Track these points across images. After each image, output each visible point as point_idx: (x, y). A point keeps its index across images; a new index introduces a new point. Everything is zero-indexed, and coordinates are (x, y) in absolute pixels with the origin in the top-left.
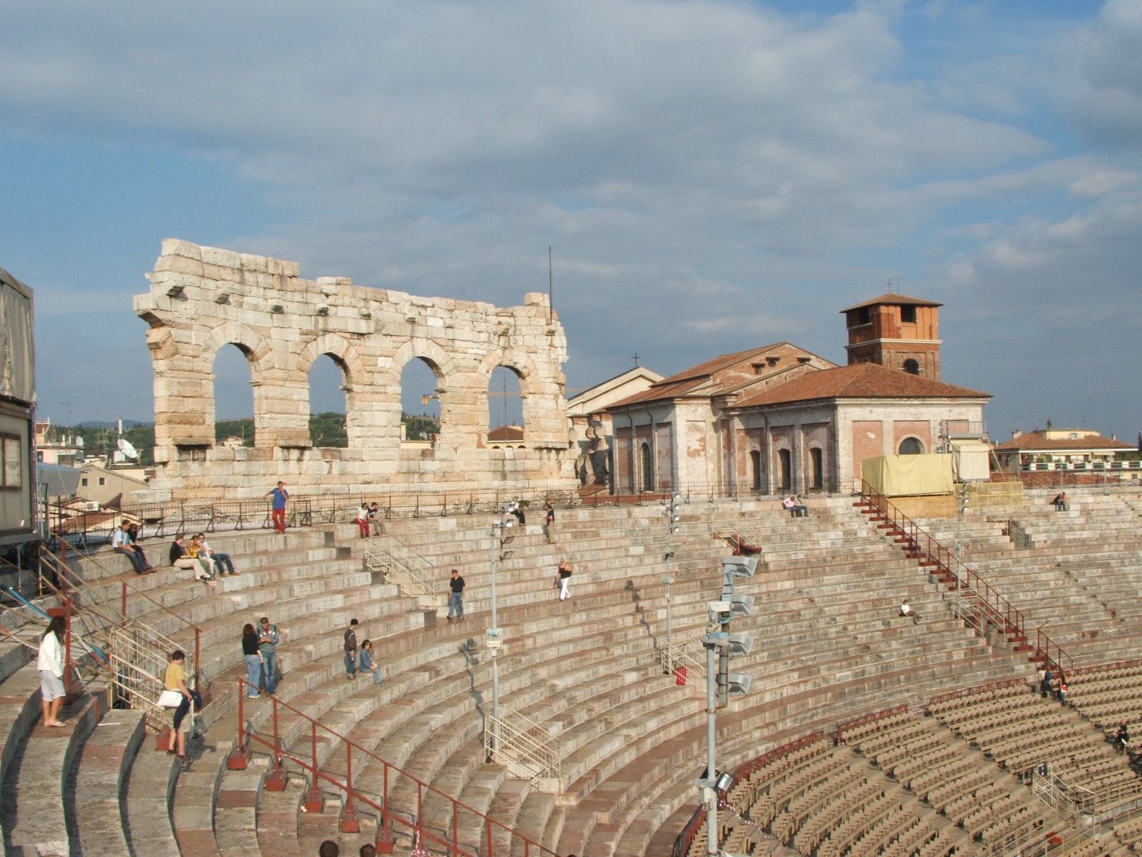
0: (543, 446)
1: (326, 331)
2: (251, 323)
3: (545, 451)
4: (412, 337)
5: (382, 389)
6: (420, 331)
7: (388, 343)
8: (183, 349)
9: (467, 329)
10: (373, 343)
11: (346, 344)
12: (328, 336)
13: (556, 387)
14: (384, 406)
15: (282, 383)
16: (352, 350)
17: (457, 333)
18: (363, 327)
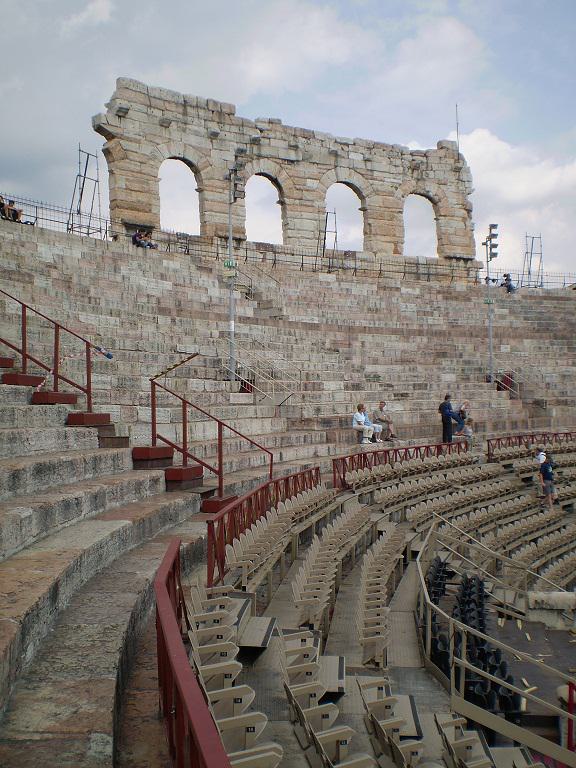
0: (452, 255)
1: (259, 156)
2: (193, 144)
3: (454, 260)
4: (336, 167)
5: (309, 203)
6: (343, 162)
7: (314, 170)
8: (132, 156)
9: (384, 163)
10: (303, 169)
11: (278, 167)
12: (262, 160)
13: (465, 212)
14: (311, 215)
15: (221, 190)
16: (284, 173)
17: (376, 166)
18: (292, 156)
